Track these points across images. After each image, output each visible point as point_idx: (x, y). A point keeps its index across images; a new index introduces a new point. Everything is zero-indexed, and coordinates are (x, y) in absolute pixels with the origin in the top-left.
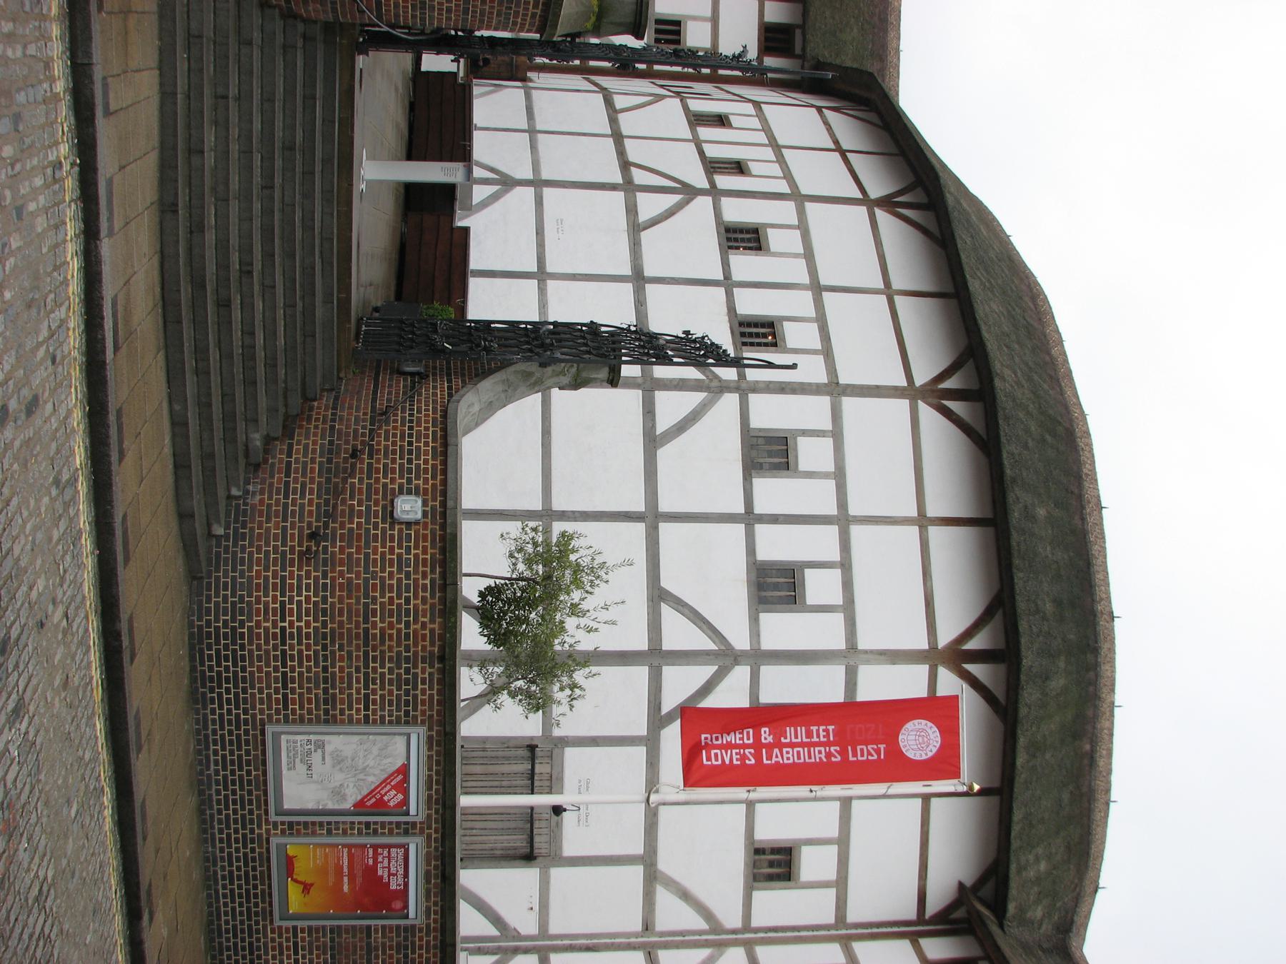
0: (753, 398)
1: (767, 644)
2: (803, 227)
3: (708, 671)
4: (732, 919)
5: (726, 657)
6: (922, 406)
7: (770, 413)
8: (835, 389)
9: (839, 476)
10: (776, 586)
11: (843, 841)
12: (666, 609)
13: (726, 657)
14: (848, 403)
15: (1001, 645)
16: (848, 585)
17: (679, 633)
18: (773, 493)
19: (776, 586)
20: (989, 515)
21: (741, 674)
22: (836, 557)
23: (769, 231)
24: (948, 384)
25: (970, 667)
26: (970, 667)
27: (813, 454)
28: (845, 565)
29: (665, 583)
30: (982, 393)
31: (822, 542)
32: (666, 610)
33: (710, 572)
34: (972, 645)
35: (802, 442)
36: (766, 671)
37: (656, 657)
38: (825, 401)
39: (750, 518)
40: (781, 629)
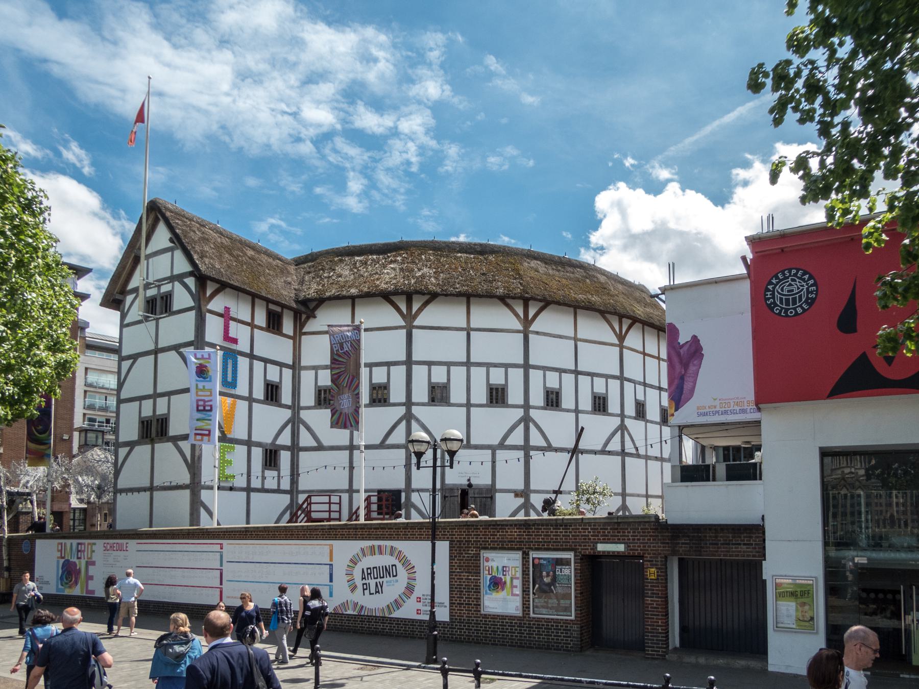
0: (414, 400)
1: (521, 402)
2: (316, 368)
3: (531, 425)
4: (617, 421)
5: (526, 420)
6: (416, 323)
7: (421, 393)
8: (409, 362)
9: (449, 364)
10: (497, 396)
11: (592, 375)
12: (507, 443)
13: (526, 420)
14: (415, 358)
15: (521, 302)
16: (496, 365)
17: (517, 438)
18: (457, 394)
19: (497, 396)
20: (465, 299)
21: (533, 413)
22: (483, 370)
23: (319, 384)
24: (405, 311)
25: (530, 317)
26: (530, 317)
27: (439, 374)
28: (488, 365)
29: (496, 441)
30: (409, 297)
31: (478, 374)
32: (507, 443)
33: (492, 424)
34: (522, 315)
35: (433, 380)
36: (532, 402)
37: (527, 448)
38: (415, 368)
39: (468, 405)
40: (515, 395)
